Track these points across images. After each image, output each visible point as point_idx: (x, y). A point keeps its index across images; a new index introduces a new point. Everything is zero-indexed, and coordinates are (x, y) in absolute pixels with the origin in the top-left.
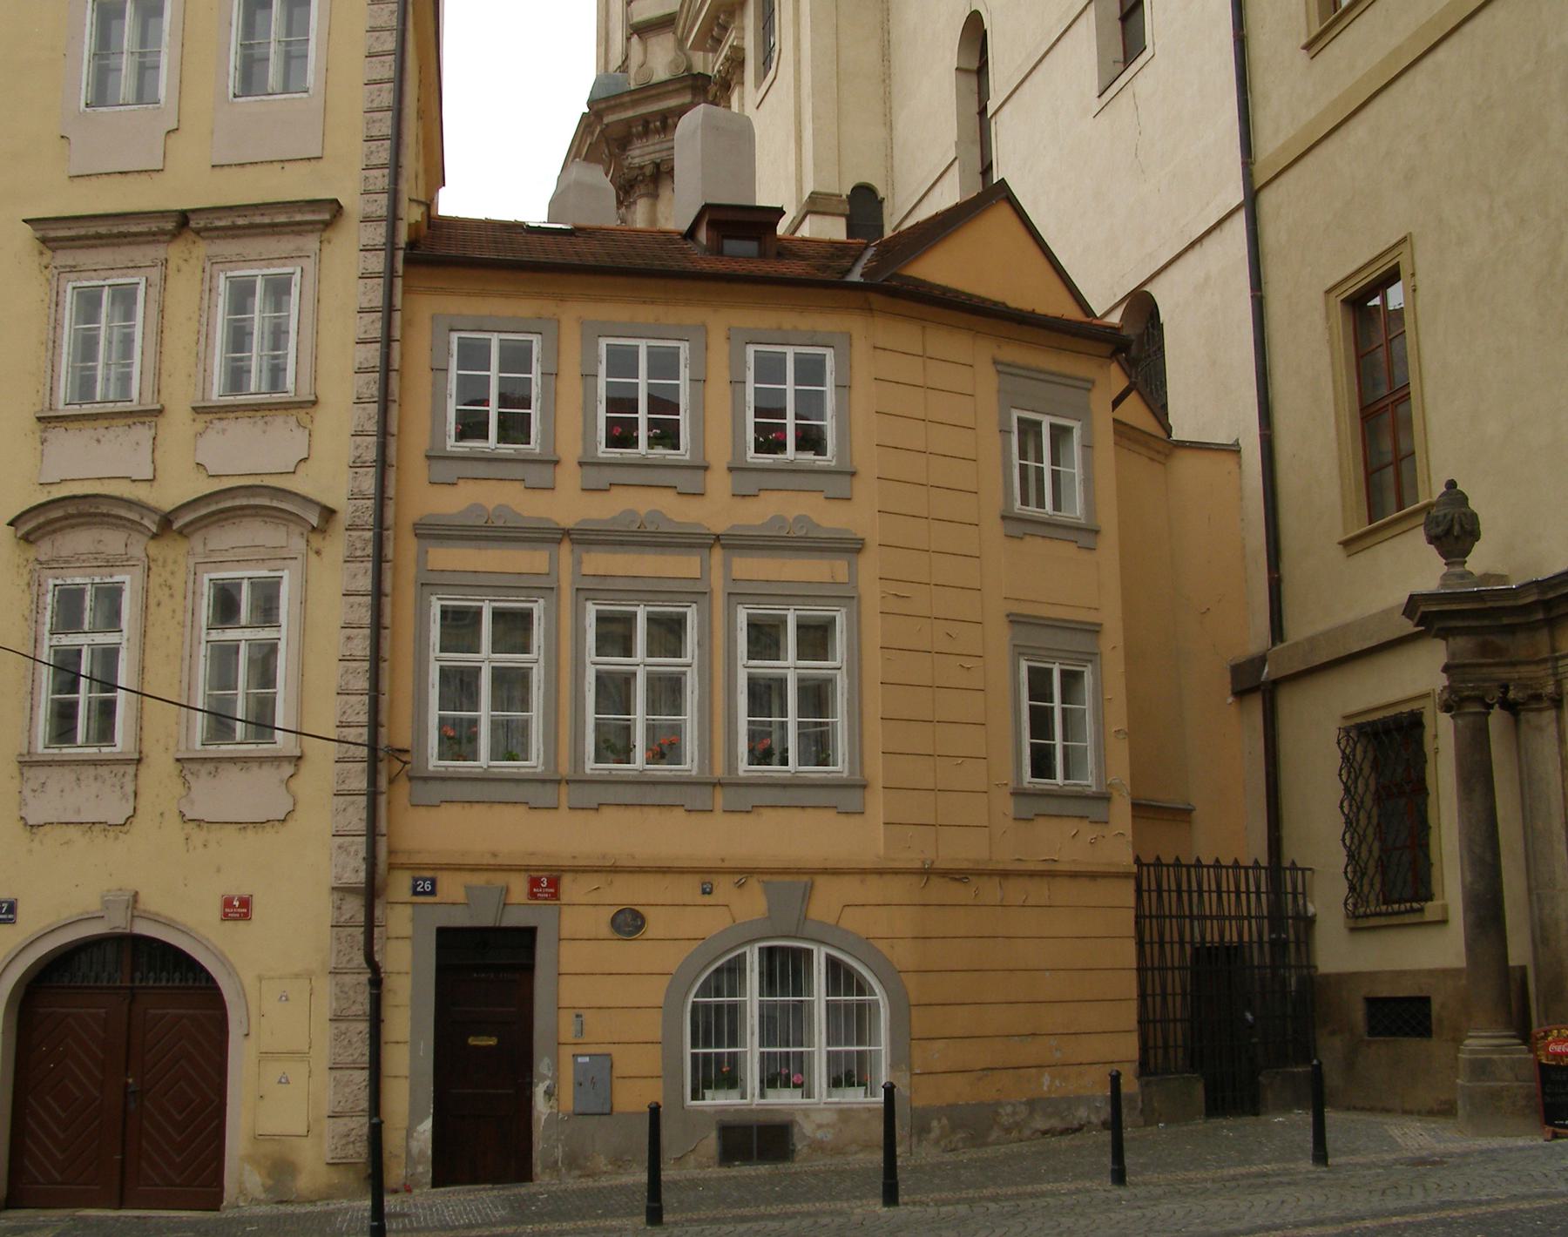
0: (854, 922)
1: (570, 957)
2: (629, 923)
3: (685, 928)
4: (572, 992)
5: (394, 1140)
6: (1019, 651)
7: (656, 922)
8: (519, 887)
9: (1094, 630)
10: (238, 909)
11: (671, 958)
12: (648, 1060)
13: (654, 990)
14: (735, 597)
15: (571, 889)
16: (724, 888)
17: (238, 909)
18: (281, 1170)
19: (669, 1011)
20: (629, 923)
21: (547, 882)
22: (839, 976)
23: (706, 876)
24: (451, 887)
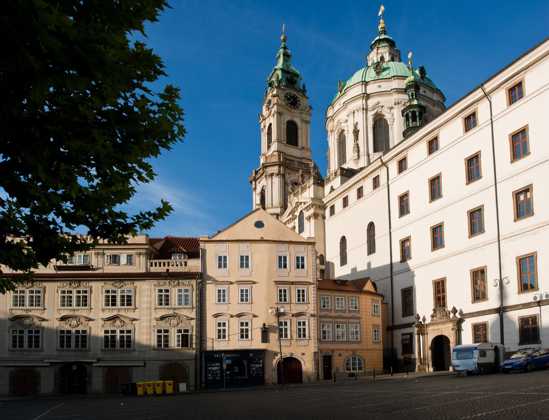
0: (360, 355)
1: (335, 358)
2: (340, 355)
3: (345, 355)
4: (335, 361)
5: (320, 376)
6: (373, 328)
7: (342, 355)
8: (330, 352)
9: (379, 326)
10: (303, 354)
11: (344, 358)
12: (342, 368)
13: (342, 361)
14: (335, 323)
15: (335, 352)
16: (349, 351)
17: (303, 354)
18: (309, 379)
19: (344, 362)
20: (340, 355)
21: (333, 351)
22: (359, 360)
23: (347, 350)
24: (324, 352)
